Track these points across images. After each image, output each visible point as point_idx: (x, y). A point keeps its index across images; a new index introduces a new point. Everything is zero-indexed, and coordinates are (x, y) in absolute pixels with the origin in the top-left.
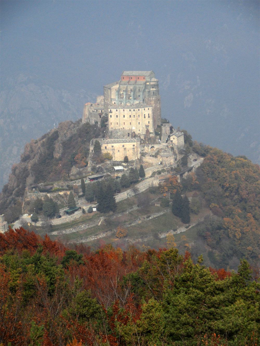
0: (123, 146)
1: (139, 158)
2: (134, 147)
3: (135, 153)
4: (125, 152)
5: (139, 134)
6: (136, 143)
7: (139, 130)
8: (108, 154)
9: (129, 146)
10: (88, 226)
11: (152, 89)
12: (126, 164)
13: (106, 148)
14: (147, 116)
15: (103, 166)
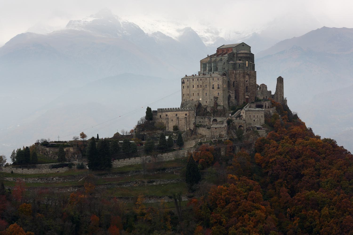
0: (176, 115)
1: (192, 129)
2: (187, 116)
3: (188, 123)
4: (178, 122)
5: (205, 105)
6: (188, 112)
7: (206, 102)
8: (162, 124)
9: (182, 115)
10: (64, 179)
11: (238, 62)
12: (176, 134)
13: (160, 116)
14: (216, 87)
15: (149, 134)
